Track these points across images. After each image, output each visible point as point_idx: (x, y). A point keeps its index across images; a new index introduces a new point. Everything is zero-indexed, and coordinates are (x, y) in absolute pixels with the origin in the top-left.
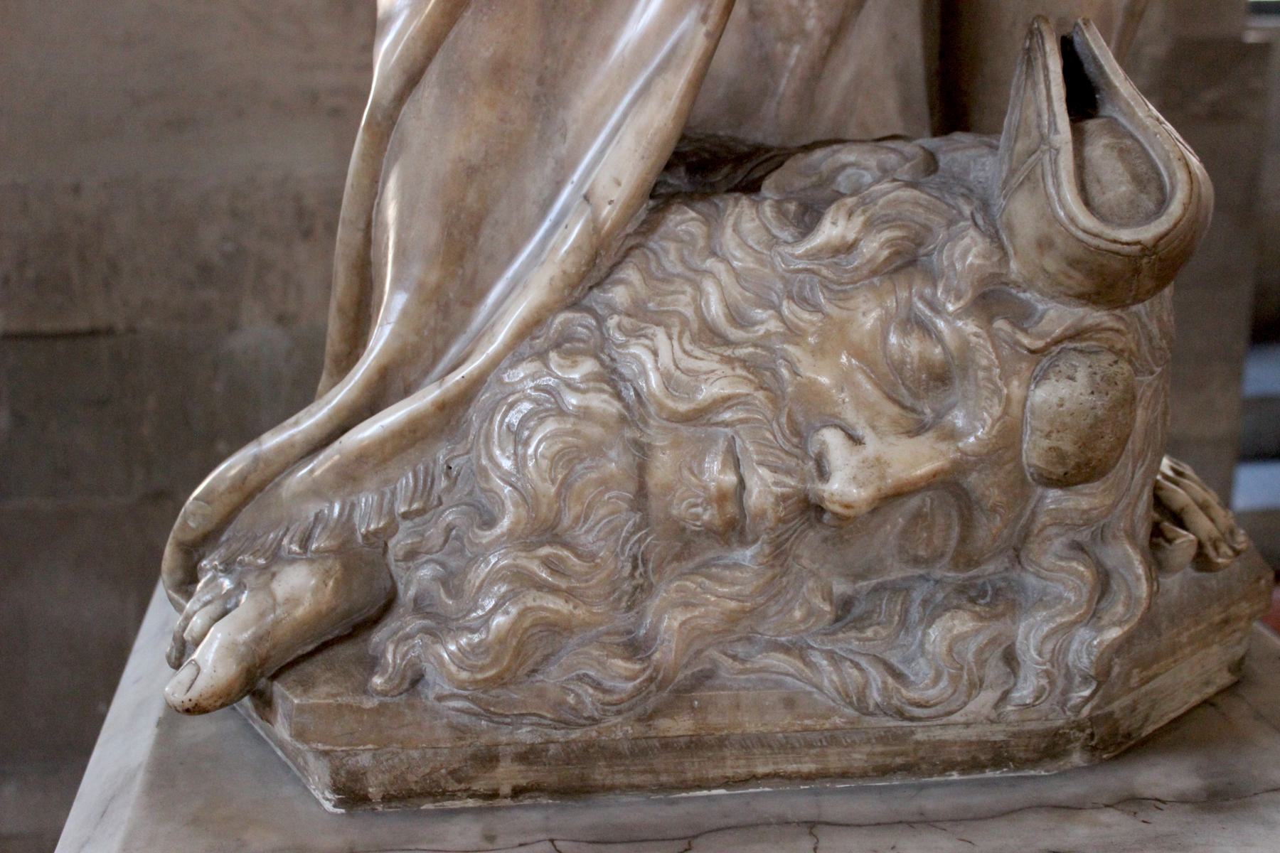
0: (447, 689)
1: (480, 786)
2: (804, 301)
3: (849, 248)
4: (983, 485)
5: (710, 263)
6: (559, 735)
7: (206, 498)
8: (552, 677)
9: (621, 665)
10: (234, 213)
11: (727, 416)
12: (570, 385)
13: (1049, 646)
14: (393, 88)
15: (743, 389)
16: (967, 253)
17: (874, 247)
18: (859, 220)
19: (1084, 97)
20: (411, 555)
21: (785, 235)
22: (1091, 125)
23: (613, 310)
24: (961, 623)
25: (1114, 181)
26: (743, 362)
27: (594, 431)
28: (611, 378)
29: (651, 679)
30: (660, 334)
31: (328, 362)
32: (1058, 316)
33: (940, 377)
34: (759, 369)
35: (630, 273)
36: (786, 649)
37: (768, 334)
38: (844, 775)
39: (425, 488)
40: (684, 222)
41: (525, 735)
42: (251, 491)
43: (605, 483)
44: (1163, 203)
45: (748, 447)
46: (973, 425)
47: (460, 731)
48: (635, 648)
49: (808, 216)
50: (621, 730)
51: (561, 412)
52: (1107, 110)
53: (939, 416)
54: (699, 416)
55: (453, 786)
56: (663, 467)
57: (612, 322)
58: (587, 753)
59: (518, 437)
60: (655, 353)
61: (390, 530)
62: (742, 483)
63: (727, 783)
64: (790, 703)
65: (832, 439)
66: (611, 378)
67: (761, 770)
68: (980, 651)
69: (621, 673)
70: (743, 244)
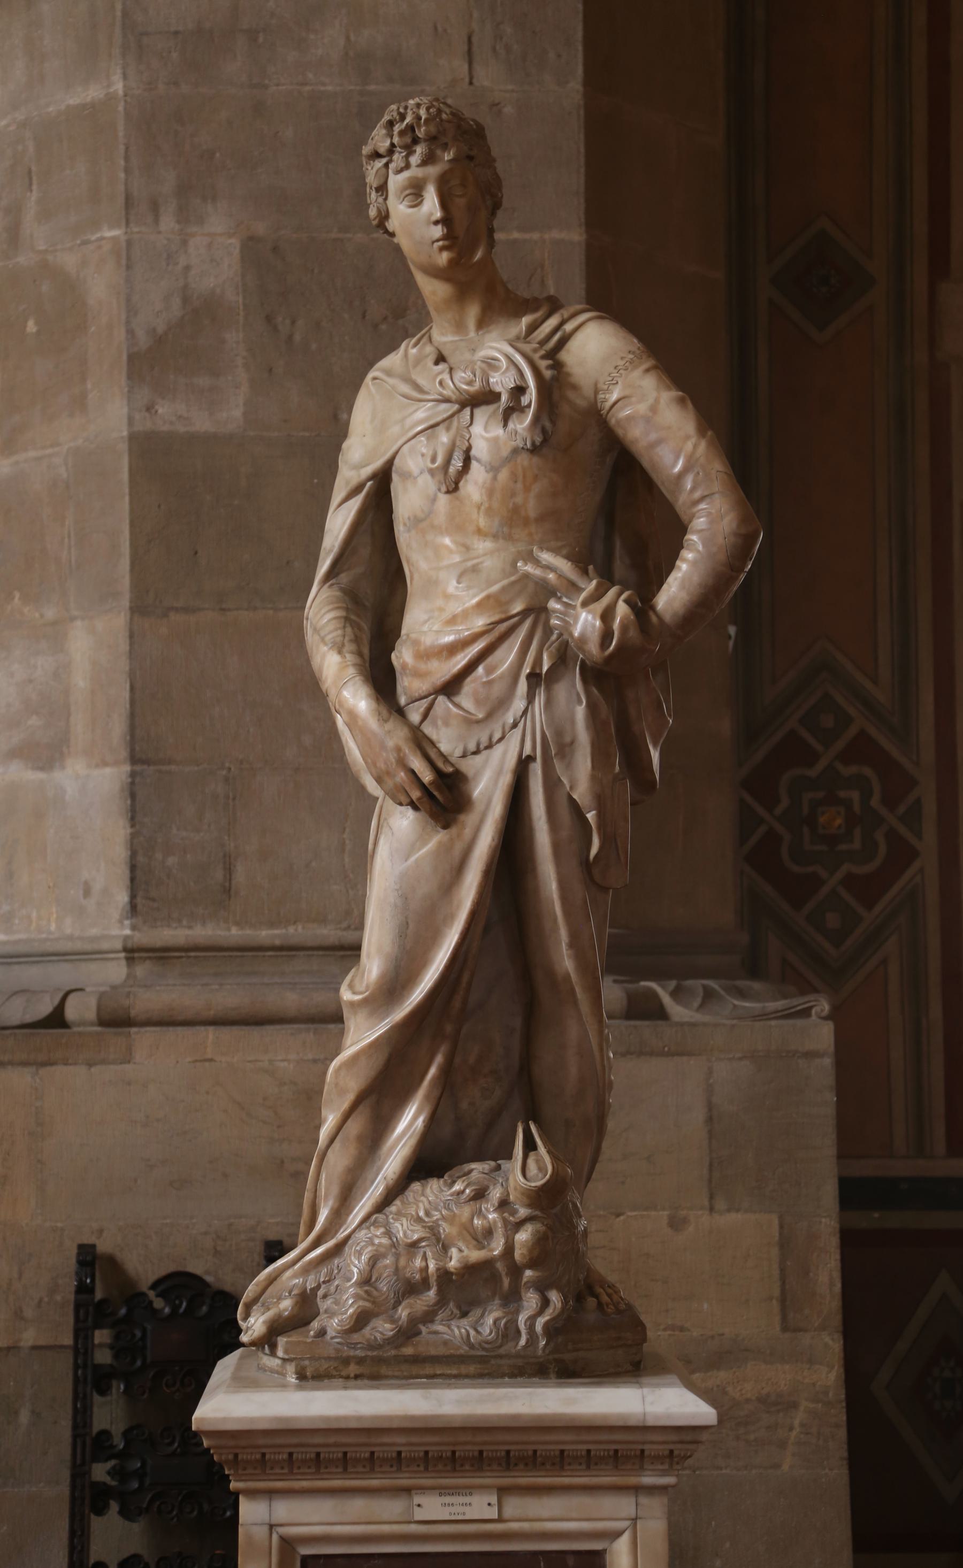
0: (334, 1334)
1: (343, 1373)
2: (448, 1209)
3: (463, 1192)
5: (422, 1198)
6: (369, 1353)
7: (257, 1285)
8: (367, 1331)
9: (388, 1326)
10: (216, 1253)
11: (424, 1244)
12: (377, 1236)
14: (325, 1143)
15: (428, 1235)
16: (496, 1194)
19: (530, 1146)
21: (445, 1189)
23: (391, 1213)
26: (429, 1227)
27: (382, 1250)
28: (389, 1233)
29: (399, 1331)
30: (404, 1220)
33: (489, 1232)
35: (398, 1202)
36: (444, 1325)
37: (437, 1220)
38: (467, 1376)
40: (416, 1186)
41: (359, 1353)
42: (272, 1280)
43: (386, 1267)
45: (429, 1254)
46: (497, 1247)
47: (337, 1351)
51: (373, 1244)
53: (489, 1244)
54: (414, 1245)
55: (335, 1373)
56: (402, 1262)
58: (380, 1361)
59: (359, 1253)
61: (318, 1287)
62: (427, 1267)
64: (446, 1343)
65: (454, 1252)
66: (389, 1233)
67: (438, 1372)
68: (506, 1324)
70: (432, 1192)
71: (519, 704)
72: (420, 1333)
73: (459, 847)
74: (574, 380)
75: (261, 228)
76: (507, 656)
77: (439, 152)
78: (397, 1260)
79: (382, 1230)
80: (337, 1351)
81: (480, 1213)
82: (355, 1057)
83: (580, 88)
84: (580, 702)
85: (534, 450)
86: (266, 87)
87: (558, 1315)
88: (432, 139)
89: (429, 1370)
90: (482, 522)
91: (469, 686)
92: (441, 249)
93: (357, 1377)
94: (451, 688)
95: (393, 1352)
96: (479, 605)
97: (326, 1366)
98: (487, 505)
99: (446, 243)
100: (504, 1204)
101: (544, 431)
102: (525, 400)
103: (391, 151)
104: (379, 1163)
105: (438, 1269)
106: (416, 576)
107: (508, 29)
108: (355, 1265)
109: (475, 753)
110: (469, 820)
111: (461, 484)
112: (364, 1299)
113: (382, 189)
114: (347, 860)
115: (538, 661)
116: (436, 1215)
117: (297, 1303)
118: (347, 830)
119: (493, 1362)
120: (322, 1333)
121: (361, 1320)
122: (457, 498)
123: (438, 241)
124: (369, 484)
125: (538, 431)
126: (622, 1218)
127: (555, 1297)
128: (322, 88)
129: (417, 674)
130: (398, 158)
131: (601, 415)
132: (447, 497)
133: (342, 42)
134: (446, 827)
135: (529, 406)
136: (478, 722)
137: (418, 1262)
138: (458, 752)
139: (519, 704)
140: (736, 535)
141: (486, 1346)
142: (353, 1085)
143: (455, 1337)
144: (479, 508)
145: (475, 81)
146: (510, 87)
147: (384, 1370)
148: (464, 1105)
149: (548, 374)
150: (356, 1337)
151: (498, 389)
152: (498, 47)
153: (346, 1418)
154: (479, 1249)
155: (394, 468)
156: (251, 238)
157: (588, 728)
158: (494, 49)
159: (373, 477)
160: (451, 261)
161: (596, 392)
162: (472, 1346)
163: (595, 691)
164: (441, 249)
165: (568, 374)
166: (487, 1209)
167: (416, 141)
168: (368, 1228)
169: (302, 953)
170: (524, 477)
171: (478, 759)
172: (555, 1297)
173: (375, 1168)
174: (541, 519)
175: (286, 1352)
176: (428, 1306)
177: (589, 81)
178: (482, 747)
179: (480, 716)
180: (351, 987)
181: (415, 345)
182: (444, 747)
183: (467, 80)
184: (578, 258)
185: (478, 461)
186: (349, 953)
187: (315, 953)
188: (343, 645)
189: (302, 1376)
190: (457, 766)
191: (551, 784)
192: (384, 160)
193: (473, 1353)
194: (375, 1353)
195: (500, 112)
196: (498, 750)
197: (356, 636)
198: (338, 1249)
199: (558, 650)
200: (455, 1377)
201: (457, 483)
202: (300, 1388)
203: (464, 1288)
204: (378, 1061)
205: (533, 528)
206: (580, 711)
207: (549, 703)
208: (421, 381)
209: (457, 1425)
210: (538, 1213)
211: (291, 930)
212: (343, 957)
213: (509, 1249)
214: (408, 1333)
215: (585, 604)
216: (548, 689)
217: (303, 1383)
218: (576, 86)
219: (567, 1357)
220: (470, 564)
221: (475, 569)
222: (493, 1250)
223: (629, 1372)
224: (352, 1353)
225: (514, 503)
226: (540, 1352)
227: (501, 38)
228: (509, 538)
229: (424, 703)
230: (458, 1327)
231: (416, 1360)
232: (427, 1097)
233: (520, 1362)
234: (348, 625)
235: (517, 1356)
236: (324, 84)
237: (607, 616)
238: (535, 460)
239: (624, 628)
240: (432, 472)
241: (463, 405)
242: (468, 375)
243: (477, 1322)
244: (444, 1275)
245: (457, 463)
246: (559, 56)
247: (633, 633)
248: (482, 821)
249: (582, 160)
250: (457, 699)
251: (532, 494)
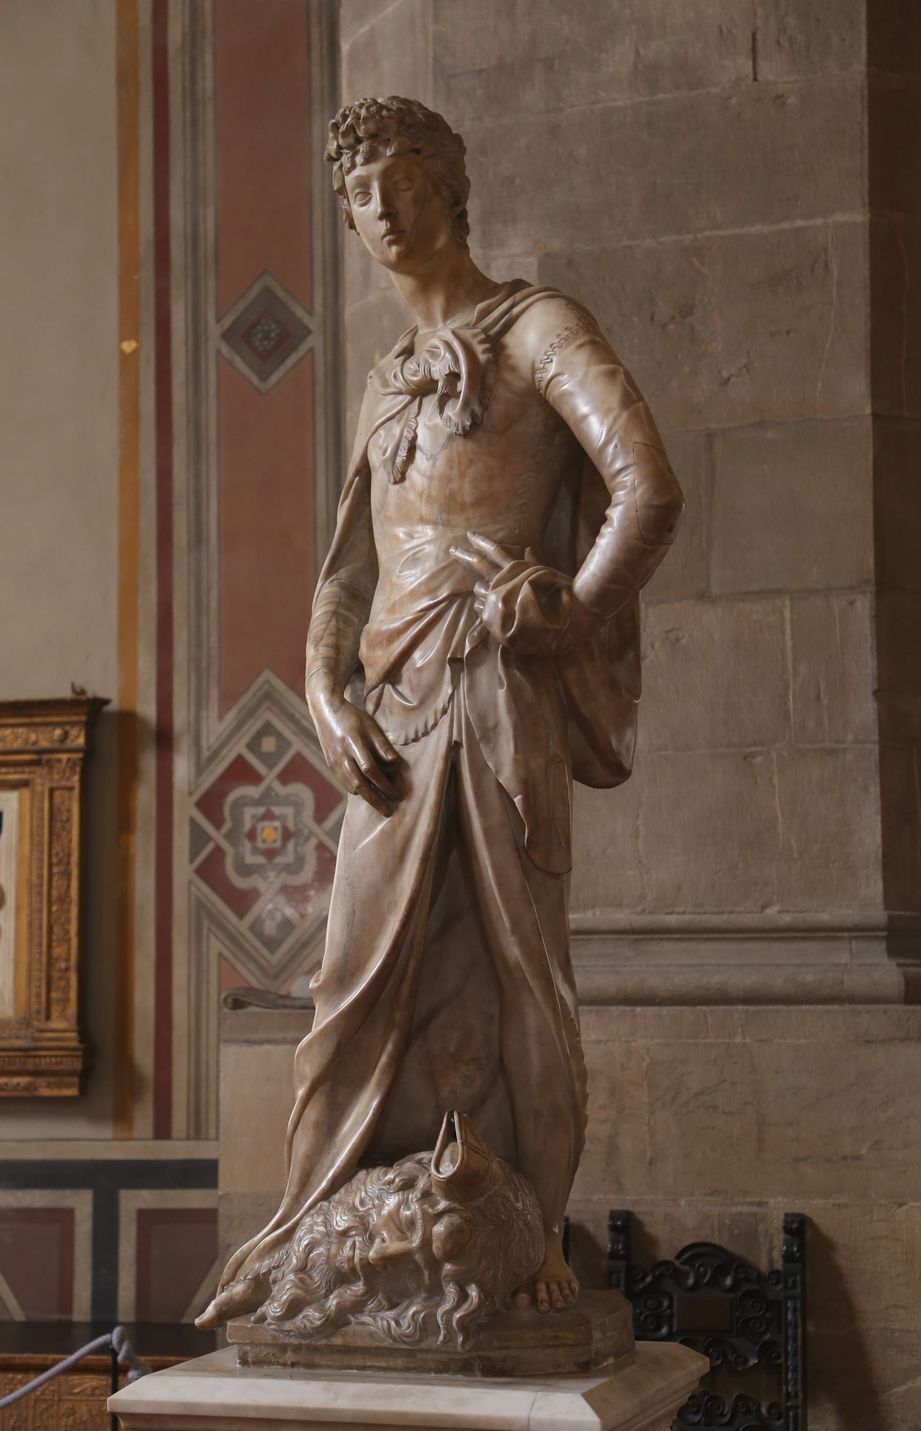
1: (281, 1361)
3: (391, 1182)
5: (362, 1187)
6: (303, 1342)
8: (299, 1320)
13: (445, 1318)
15: (356, 1224)
19: (450, 1136)
28: (326, 1223)
29: (326, 1320)
33: (411, 1223)
35: (342, 1190)
36: (370, 1316)
38: (395, 1369)
40: (362, 1174)
47: (274, 1337)
55: (273, 1360)
59: (300, 1240)
64: (371, 1335)
66: (326, 1223)
67: (368, 1364)
72: (348, 1323)
73: (401, 833)
74: (512, 362)
75: (556, 245)
77: (381, 149)
78: (329, 1250)
80: (274, 1337)
83: (864, 68)
84: (501, 685)
85: (467, 434)
86: (561, 110)
87: (474, 1311)
88: (373, 136)
89: (359, 1361)
90: (424, 510)
91: (407, 672)
92: (390, 243)
93: (293, 1365)
95: (324, 1342)
97: (265, 1353)
98: (426, 493)
100: (426, 1195)
101: (473, 416)
103: (339, 153)
104: (334, 1150)
105: (361, 1260)
107: (792, 21)
109: (416, 740)
110: (409, 807)
114: (641, 846)
117: (249, 1287)
118: (641, 816)
119: (419, 1356)
121: (294, 1308)
122: (404, 488)
123: (385, 236)
124: (357, 479)
125: (468, 415)
126: (905, 1208)
127: (473, 1292)
128: (613, 104)
130: (345, 160)
131: (541, 395)
132: (397, 487)
133: (631, 57)
134: (388, 815)
136: (413, 709)
137: (347, 1251)
138: (402, 741)
139: (447, 689)
140: (648, 506)
141: (406, 1339)
143: (377, 1328)
144: (421, 497)
145: (759, 77)
146: (793, 78)
147: (318, 1359)
148: (445, 1093)
149: (482, 357)
150: (288, 1325)
152: (781, 41)
153: (245, 1407)
154: (402, 1240)
156: (547, 255)
157: (509, 711)
158: (778, 43)
160: (399, 255)
161: (534, 371)
163: (518, 674)
164: (390, 243)
165: (509, 357)
167: (359, 141)
168: (312, 1215)
169: (597, 937)
170: (459, 463)
172: (473, 1292)
173: (330, 1157)
174: (477, 503)
176: (356, 1296)
177: (873, 60)
178: (420, 734)
179: (415, 703)
182: (391, 737)
183: (751, 77)
184: (862, 239)
185: (421, 450)
186: (641, 936)
187: (610, 936)
188: (322, 638)
189: (244, 1362)
190: (400, 754)
194: (307, 1342)
195: (784, 103)
197: (338, 630)
198: (289, 1235)
199: (480, 634)
200: (385, 1369)
202: (243, 1375)
203: (388, 1277)
205: (470, 513)
206: (502, 694)
207: (471, 687)
209: (347, 1420)
210: (455, 1205)
211: (589, 914)
212: (636, 940)
213: (427, 1242)
214: (336, 1322)
216: (471, 673)
217: (246, 1368)
218: (859, 67)
219: (496, 1355)
222: (411, 1242)
223: (573, 1373)
224: (287, 1340)
225: (450, 490)
226: (460, 1349)
227: (785, 31)
228: (447, 524)
229: (375, 692)
230: (382, 1319)
231: (348, 1350)
232: (378, 1085)
233: (445, 1358)
234: (334, 619)
235: (438, 1351)
236: (614, 100)
237: (508, 599)
238: (470, 444)
239: (524, 609)
243: (399, 1315)
244: (367, 1265)
245: (403, 453)
246: (843, 40)
247: (533, 613)
248: (421, 808)
249: (866, 139)
250: (400, 688)
251: (467, 479)
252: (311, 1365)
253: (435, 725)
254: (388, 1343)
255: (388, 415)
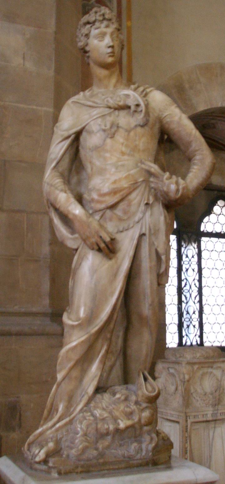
1: (76, 471)
2: (115, 404)
3: (119, 398)
4: (137, 426)
9: (95, 452)
16: (134, 398)
17: (123, 398)
18: (121, 395)
19: (145, 379)
20: (66, 441)
21: (111, 397)
22: (147, 383)
24: (135, 444)
25: (150, 388)
27: (91, 422)
28: (93, 415)
30: (98, 410)
31: (43, 418)
32: (144, 405)
33: (131, 413)
34: (110, 413)
36: (114, 449)
38: (121, 468)
39: (67, 431)
40: (99, 396)
41: (82, 463)
42: (41, 434)
44: (155, 391)
46: (136, 419)
48: (97, 449)
49: (114, 394)
50: (94, 461)
52: (148, 380)
54: (103, 419)
56: (99, 426)
57: (91, 408)
60: (98, 411)
62: (109, 427)
63: (107, 470)
64: (115, 457)
65: (120, 421)
67: (111, 467)
69: (95, 453)
71: (139, 215)
76: (135, 197)
77: (111, 25)
79: (89, 414)
81: (127, 406)
82: (75, 347)
91: (122, 206)
92: (110, 56)
93: (81, 472)
94: (113, 207)
96: (126, 177)
99: (111, 54)
102: (139, 109)
106: (94, 168)
108: (80, 427)
109: (122, 232)
110: (120, 255)
111: (116, 135)
112: (85, 442)
113: (87, 36)
115: (148, 199)
116: (111, 407)
120: (68, 456)
123: (109, 53)
129: (98, 202)
130: (97, 24)
134: (111, 259)
135: (141, 111)
138: (116, 231)
142: (75, 357)
151: (130, 104)
155: (85, 130)
159: (75, 133)
162: (124, 457)
166: (131, 405)
167: (104, 19)
171: (123, 234)
174: (144, 151)
175: (54, 464)
179: (125, 218)
180: (69, 319)
181: (88, 92)
189: (60, 473)
191: (151, 244)
192: (91, 25)
193: (124, 459)
196: (130, 232)
201: (114, 134)
204: (85, 348)
206: (162, 218)
208: (99, 102)
213: (140, 420)
214: (101, 455)
215: (167, 179)
220: (120, 163)
221: (123, 166)
224: (80, 463)
231: (105, 464)
232: (101, 361)
235: (140, 459)
237: (177, 183)
240: (104, 131)
241: (115, 109)
242: (118, 99)
244: (117, 431)
252: (88, 472)
253: (133, 227)
254: (122, 458)
255: (103, 114)
